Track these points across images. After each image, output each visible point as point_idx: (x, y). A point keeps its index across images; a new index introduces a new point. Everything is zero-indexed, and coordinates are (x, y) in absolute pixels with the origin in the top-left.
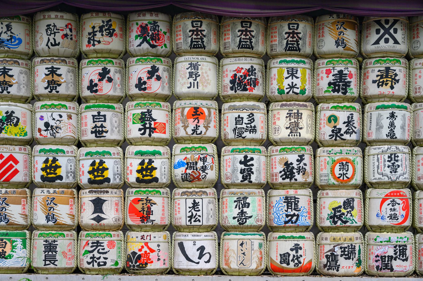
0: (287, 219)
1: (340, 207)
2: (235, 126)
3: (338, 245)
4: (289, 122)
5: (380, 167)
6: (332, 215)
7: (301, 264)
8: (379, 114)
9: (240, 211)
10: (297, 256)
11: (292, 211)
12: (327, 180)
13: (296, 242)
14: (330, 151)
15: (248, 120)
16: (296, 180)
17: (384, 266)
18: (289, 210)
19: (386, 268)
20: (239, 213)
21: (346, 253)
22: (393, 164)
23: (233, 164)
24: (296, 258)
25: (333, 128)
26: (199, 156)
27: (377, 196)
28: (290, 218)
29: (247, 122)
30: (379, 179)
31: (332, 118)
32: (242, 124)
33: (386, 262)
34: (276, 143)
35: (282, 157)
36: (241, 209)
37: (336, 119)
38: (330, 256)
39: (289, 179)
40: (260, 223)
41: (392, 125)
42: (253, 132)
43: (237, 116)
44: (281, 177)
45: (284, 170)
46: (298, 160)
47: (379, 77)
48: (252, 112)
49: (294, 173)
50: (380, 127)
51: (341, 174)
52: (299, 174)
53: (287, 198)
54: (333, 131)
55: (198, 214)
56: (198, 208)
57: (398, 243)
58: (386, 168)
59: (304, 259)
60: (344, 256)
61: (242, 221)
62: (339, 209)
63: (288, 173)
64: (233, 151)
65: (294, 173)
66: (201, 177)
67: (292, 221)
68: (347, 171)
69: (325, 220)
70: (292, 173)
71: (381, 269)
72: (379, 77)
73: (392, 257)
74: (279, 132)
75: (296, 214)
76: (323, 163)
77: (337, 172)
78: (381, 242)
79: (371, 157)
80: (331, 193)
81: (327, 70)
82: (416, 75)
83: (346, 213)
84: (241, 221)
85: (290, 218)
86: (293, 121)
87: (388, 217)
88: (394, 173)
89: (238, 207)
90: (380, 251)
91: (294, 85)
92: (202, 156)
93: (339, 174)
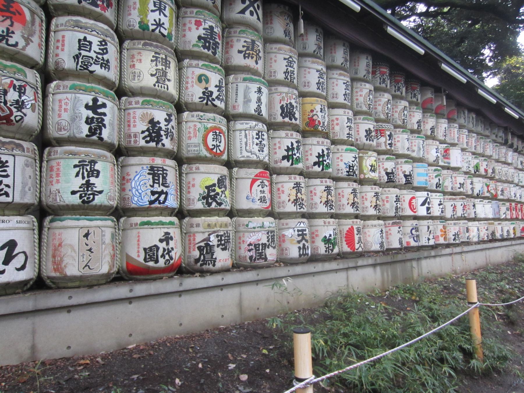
0: (153, 198)
1: (214, 185)
2: (77, 52)
3: (214, 232)
4: (155, 68)
5: (248, 144)
6: (205, 195)
7: (173, 261)
8: (247, 86)
9: (84, 182)
10: (168, 249)
11: (159, 186)
12: (197, 150)
13: (166, 230)
14: (201, 116)
15: (100, 49)
16: (163, 145)
17: (258, 256)
18: (156, 185)
19: (261, 258)
20: (83, 184)
21: (223, 242)
22: (261, 142)
23: (74, 108)
24: (166, 252)
25: (205, 90)
26: (12, 82)
27: (246, 176)
28: (156, 196)
29: (98, 51)
30: (248, 157)
31: (203, 78)
32: (89, 51)
33: (261, 251)
34: (134, 93)
35: (145, 112)
36: (86, 179)
37: (207, 81)
38: (204, 247)
39: (155, 143)
40: (112, 203)
41: (259, 100)
42: (105, 68)
43: (82, 38)
44: (144, 138)
45: (148, 130)
46: (166, 120)
47: (245, 48)
48: (105, 38)
49: (162, 136)
50: (247, 101)
51: (214, 145)
52: (167, 138)
53: (152, 168)
54: (204, 93)
55: (4, 183)
56: (5, 171)
57: (270, 229)
58: (255, 145)
59: (176, 253)
60: (221, 247)
61: (88, 198)
62: (213, 188)
63: (153, 135)
64: (74, 87)
65: (162, 136)
66: (12, 118)
67: (159, 201)
68: (220, 142)
69: (195, 201)
70: (159, 136)
71: (255, 260)
72: (245, 48)
73: (265, 244)
74: (141, 78)
75: (165, 191)
76: (191, 130)
77: (210, 142)
78: (254, 228)
79: (238, 133)
80: (203, 167)
81: (196, 21)
82: (271, 59)
83: (220, 193)
84: (85, 198)
85: (156, 196)
86: (160, 67)
87: (259, 200)
88: (261, 152)
89: (80, 175)
90: (253, 238)
91: (161, 23)
92: (17, 83)
93: (213, 145)
